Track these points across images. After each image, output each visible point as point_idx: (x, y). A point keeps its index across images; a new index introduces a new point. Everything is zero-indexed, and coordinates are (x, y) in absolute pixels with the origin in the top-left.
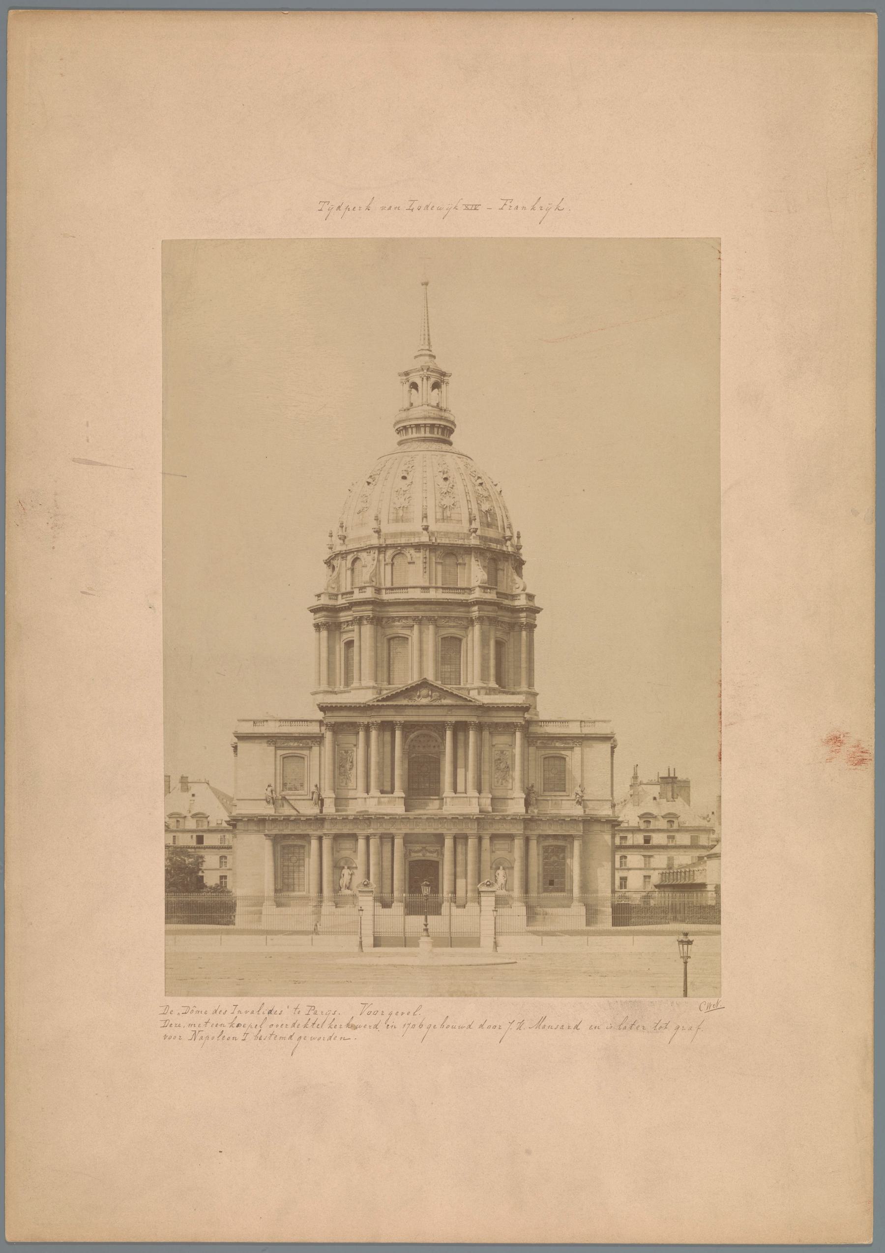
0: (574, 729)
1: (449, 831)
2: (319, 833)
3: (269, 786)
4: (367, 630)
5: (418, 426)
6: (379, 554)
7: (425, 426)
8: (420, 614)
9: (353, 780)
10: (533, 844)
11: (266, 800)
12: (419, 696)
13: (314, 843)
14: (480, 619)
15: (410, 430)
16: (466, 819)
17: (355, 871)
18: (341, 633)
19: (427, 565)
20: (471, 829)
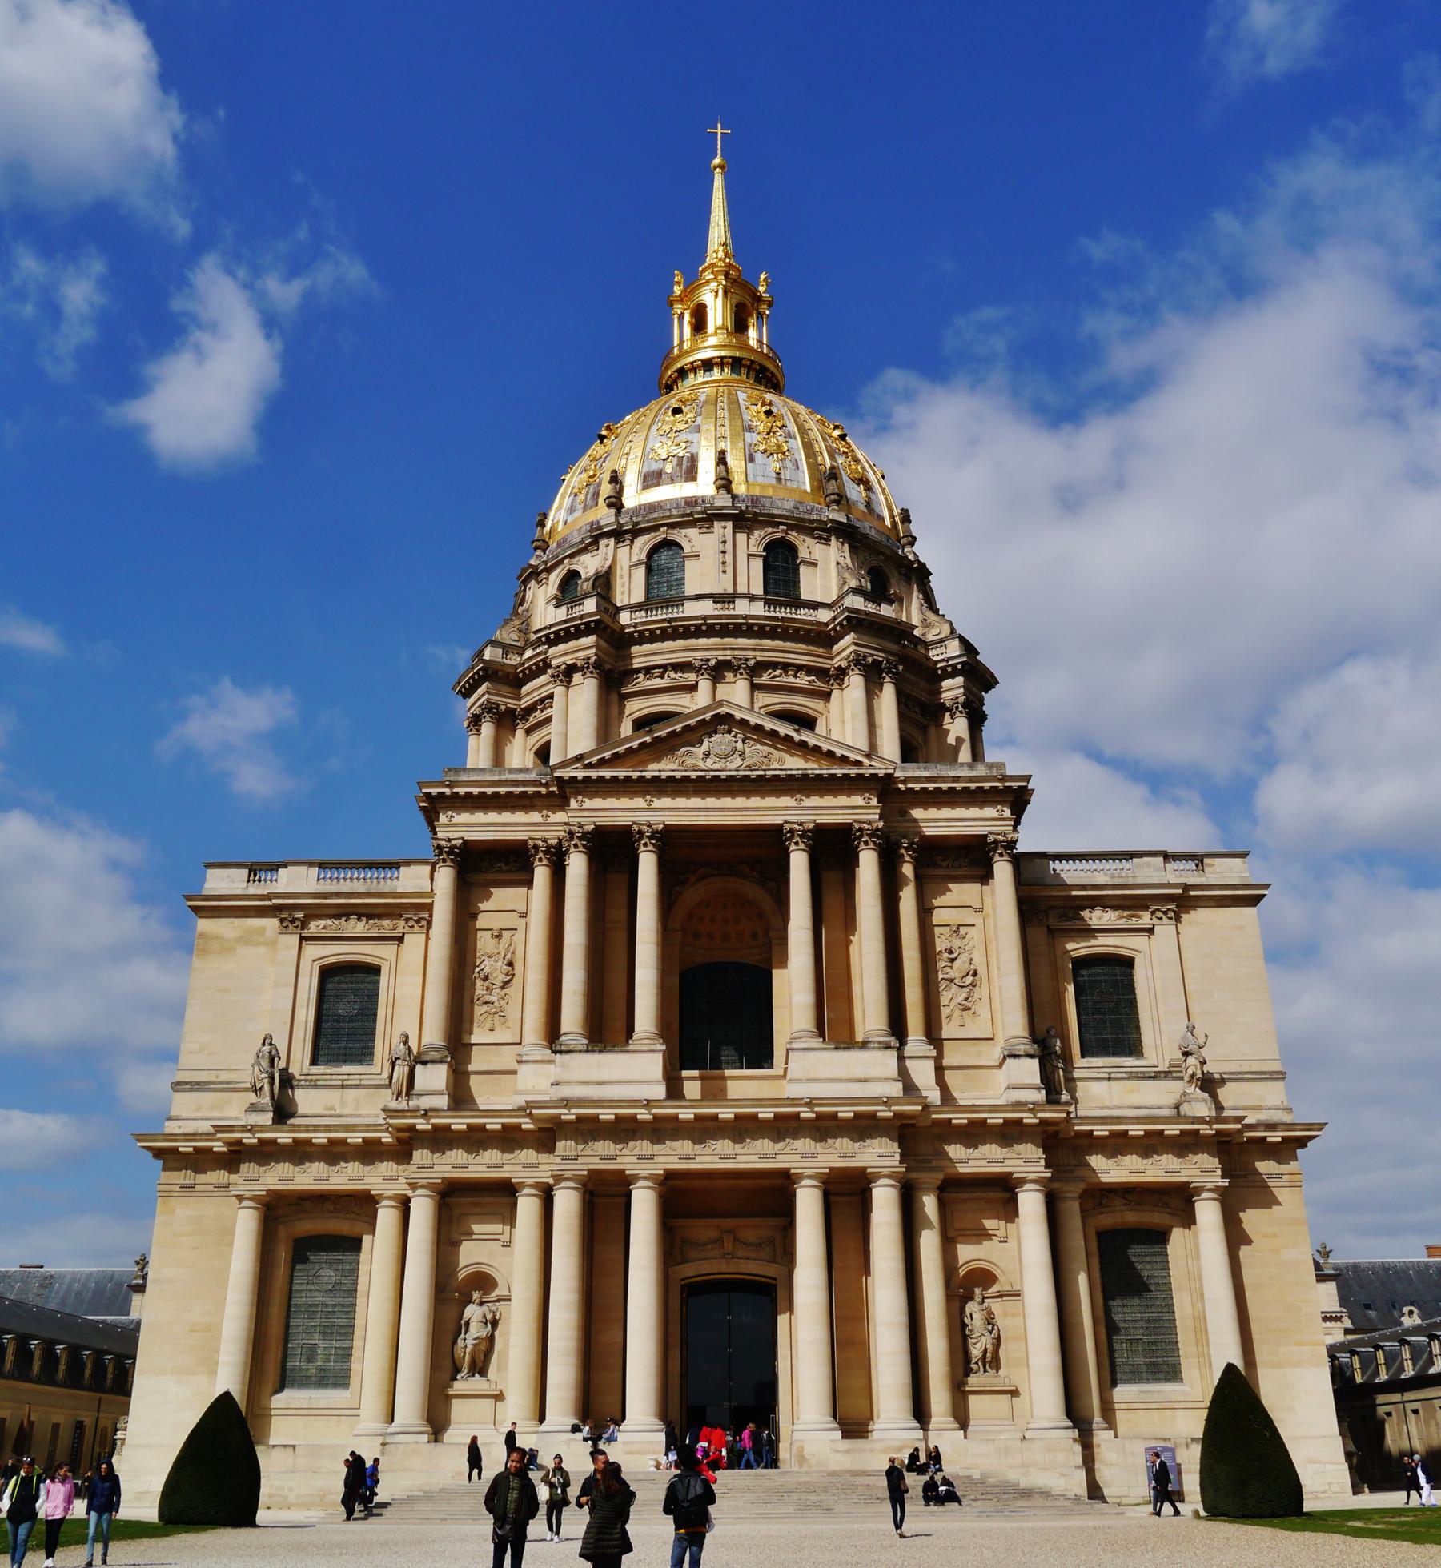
0: (1150, 874)
1: (807, 1160)
2: (401, 1187)
3: (268, 1040)
4: (585, 690)
5: (708, 365)
6: (616, 548)
7: (722, 362)
8: (715, 656)
9: (512, 1012)
10: (1072, 1210)
11: (257, 1090)
12: (707, 754)
13: (387, 1217)
14: (858, 661)
15: (692, 375)
16: (864, 1126)
17: (501, 1307)
18: (528, 732)
19: (729, 558)
20: (879, 1155)
